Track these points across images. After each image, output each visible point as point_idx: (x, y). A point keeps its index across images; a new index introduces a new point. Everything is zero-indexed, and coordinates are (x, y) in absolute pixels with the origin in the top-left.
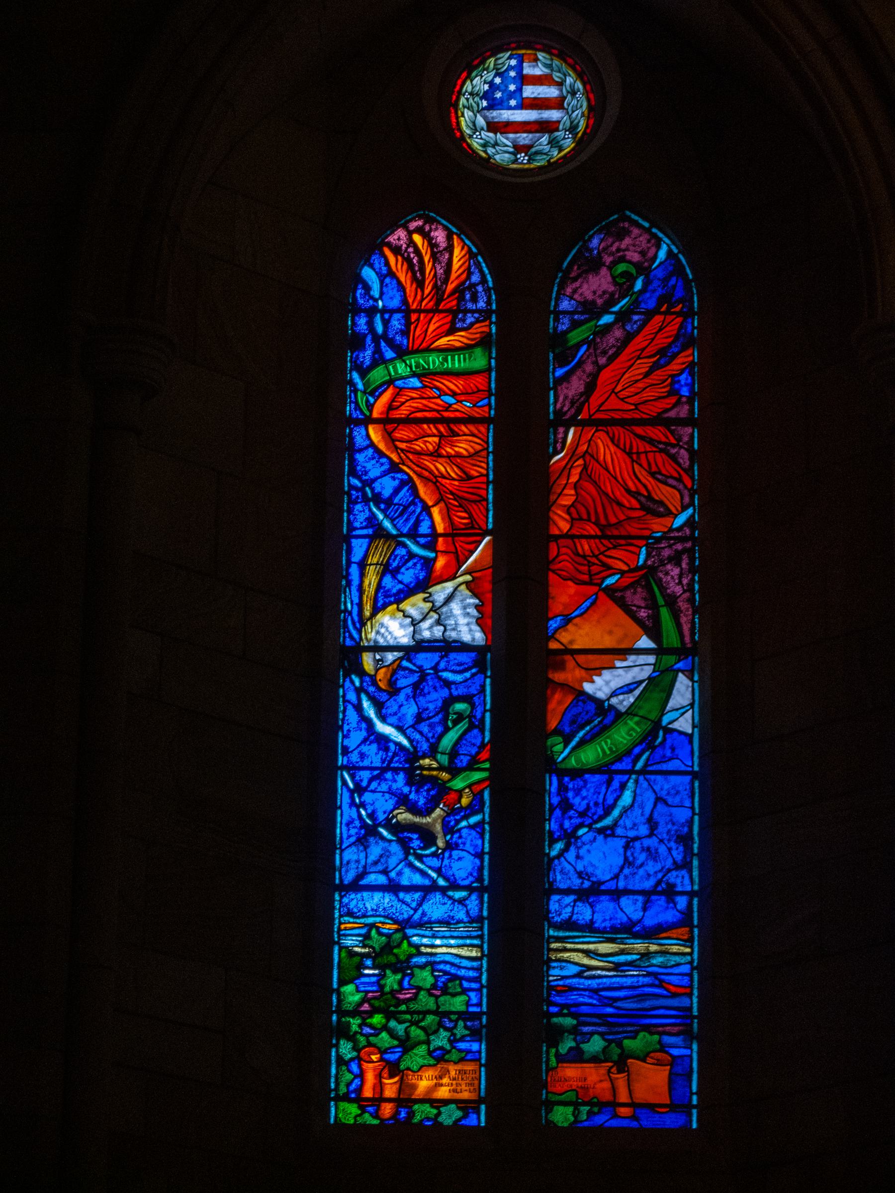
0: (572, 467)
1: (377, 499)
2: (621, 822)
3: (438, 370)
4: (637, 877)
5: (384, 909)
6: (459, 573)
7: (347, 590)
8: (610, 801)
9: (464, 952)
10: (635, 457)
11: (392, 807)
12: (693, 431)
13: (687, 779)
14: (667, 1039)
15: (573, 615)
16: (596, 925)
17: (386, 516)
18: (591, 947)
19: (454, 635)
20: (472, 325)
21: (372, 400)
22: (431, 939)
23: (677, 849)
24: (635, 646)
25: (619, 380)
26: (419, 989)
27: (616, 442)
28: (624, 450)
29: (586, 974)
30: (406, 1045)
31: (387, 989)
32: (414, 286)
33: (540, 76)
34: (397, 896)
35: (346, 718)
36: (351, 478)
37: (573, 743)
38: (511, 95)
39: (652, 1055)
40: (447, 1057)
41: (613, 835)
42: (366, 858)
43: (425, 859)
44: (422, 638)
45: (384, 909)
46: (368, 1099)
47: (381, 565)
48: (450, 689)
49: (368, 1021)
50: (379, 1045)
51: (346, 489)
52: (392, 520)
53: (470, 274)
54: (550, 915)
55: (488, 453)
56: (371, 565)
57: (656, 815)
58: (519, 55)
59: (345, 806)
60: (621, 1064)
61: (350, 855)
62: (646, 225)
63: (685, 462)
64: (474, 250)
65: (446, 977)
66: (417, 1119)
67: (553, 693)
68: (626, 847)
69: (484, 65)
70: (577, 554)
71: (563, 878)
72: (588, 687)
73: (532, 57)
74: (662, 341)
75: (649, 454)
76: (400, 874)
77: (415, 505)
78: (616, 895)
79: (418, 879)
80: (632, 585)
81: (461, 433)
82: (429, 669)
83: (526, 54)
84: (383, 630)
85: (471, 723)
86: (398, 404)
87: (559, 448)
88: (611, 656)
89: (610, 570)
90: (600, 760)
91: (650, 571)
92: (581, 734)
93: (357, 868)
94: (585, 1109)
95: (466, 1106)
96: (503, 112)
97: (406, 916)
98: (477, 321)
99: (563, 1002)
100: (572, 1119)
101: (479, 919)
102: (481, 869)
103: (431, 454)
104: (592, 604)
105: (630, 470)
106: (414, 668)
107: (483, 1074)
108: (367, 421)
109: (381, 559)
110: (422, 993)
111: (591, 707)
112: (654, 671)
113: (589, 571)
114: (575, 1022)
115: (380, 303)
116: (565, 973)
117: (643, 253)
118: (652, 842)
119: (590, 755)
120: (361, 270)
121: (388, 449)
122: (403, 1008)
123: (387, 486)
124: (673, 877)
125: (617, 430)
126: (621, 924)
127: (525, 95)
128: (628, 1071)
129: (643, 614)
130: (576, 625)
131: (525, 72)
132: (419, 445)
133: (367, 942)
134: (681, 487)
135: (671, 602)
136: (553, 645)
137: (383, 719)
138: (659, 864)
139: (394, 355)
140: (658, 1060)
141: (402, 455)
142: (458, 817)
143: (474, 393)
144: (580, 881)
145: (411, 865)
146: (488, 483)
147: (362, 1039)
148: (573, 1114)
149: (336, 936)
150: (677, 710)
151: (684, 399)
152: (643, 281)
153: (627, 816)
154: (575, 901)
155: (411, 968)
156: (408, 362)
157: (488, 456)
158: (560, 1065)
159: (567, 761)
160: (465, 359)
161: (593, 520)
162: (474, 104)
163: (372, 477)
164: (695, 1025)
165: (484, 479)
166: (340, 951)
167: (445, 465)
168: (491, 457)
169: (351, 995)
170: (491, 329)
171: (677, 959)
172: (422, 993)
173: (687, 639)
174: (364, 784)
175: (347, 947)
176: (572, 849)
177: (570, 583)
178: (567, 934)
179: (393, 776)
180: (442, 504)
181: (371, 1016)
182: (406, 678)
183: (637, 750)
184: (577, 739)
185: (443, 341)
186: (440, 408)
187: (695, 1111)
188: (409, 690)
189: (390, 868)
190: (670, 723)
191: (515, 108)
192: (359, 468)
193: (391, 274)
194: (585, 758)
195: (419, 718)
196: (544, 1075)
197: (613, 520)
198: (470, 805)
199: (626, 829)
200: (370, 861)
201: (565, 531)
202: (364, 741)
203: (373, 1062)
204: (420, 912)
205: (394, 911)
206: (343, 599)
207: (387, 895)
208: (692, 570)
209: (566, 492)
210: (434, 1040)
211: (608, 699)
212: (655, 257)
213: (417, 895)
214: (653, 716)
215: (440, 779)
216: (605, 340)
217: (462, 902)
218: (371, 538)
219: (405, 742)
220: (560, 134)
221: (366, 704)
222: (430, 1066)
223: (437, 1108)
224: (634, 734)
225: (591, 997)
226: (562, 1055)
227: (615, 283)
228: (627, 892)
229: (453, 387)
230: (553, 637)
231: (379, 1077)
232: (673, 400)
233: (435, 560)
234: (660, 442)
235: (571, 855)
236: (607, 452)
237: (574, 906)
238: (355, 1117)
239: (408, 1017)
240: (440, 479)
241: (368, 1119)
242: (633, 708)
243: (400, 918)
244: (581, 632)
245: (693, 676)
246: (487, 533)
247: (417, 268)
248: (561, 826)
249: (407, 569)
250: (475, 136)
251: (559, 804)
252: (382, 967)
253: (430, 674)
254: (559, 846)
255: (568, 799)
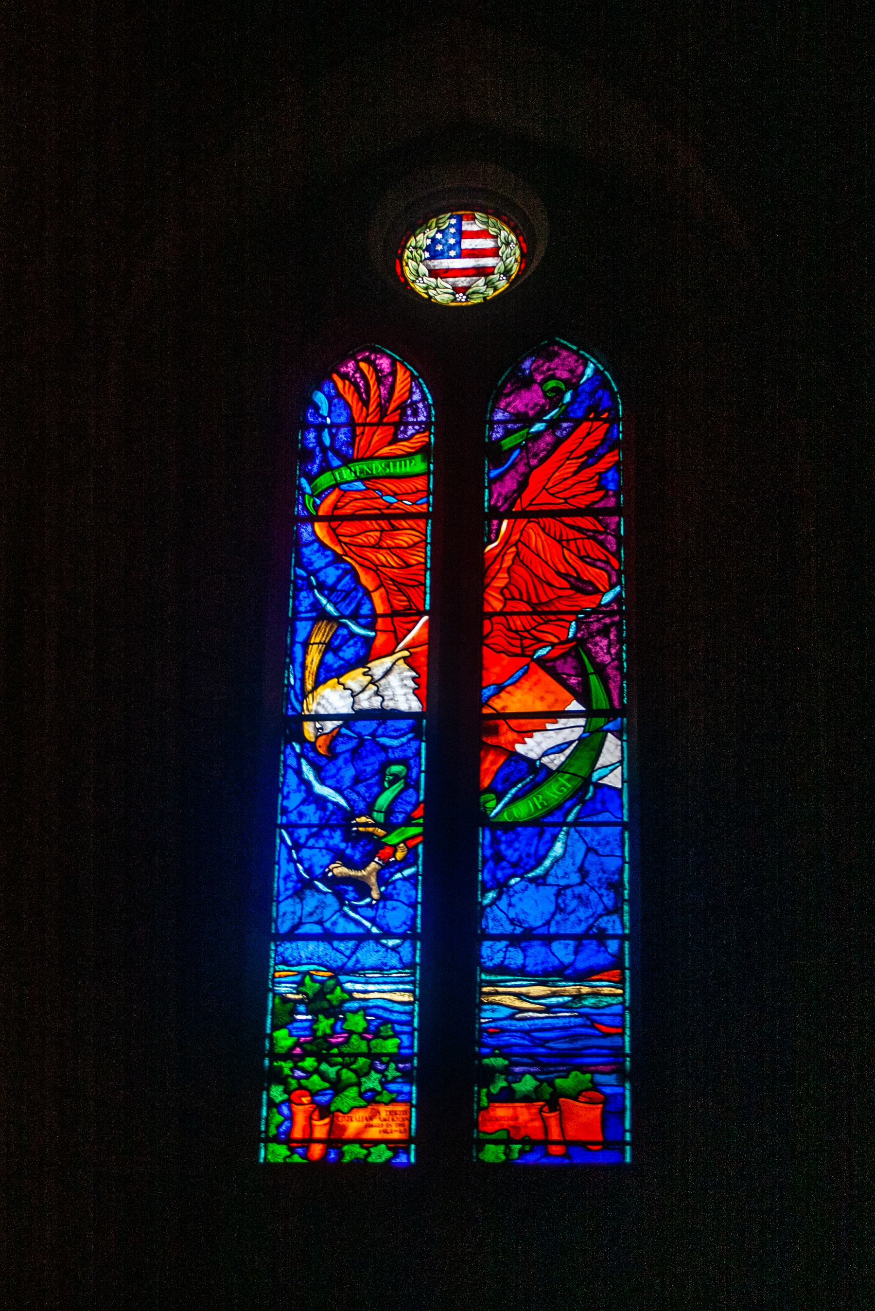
0: (505, 553)
1: (322, 586)
2: (553, 871)
3: (381, 475)
4: (569, 923)
5: (319, 957)
6: (397, 650)
7: (291, 667)
8: (542, 852)
9: (397, 997)
10: (564, 543)
11: (328, 862)
12: (620, 520)
13: (618, 829)
14: (599, 1078)
15: (506, 684)
16: (528, 969)
17: (329, 601)
18: (523, 990)
19: (389, 705)
20: (412, 435)
21: (318, 501)
22: (363, 985)
23: (608, 895)
24: (566, 709)
25: (549, 479)
26: (351, 1033)
27: (547, 531)
28: (555, 538)
29: (518, 1016)
30: (337, 1087)
31: (319, 1033)
32: (360, 405)
33: (478, 231)
34: (332, 945)
35: (287, 781)
36: (296, 569)
37: (506, 799)
38: (451, 247)
39: (584, 1093)
40: (378, 1098)
41: (545, 884)
42: (302, 909)
43: (359, 910)
44: (361, 708)
45: (319, 957)
46: (297, 1141)
47: (324, 643)
48: (387, 753)
49: (300, 1064)
50: (310, 1087)
51: (292, 578)
52: (335, 605)
53: (411, 393)
54: (483, 960)
55: (427, 544)
56: (314, 643)
57: (586, 864)
58: (459, 215)
59: (283, 862)
60: (553, 1103)
61: (286, 906)
62: (575, 348)
63: (612, 547)
64: (416, 373)
65: (379, 1021)
66: (347, 1159)
67: (486, 755)
68: (558, 895)
69: (427, 224)
70: (510, 629)
71: (495, 925)
72: (520, 748)
73: (470, 217)
74: (590, 444)
75: (578, 541)
76: (334, 923)
77: (357, 592)
78: (548, 940)
79: (352, 928)
80: (563, 656)
81: (401, 527)
82: (367, 735)
83: (464, 214)
84: (323, 702)
85: (406, 783)
86: (343, 504)
87: (493, 538)
88: (543, 720)
89: (543, 643)
90: (533, 814)
91: (580, 642)
92: (513, 791)
93: (293, 919)
94: (517, 1147)
95: (397, 1147)
96: (442, 261)
97: (340, 963)
98: (418, 432)
99: (495, 1043)
100: (503, 1157)
101: (412, 965)
102: (414, 917)
103: (373, 547)
104: (524, 674)
105: (561, 553)
106: (353, 735)
107: (414, 1114)
108: (311, 519)
109: (324, 639)
110: (354, 1038)
111: (523, 766)
112: (584, 732)
113: (522, 644)
114: (506, 1062)
115: (328, 421)
116: (496, 1015)
117: (571, 371)
118: (583, 890)
119: (522, 810)
120: (311, 393)
121: (333, 542)
122: (335, 1051)
123: (331, 575)
124: (604, 922)
125: (548, 521)
126: (553, 967)
127: (463, 247)
128: (560, 1110)
129: (573, 681)
130: (509, 693)
131: (464, 228)
132: (361, 539)
133: (302, 989)
134: (609, 568)
135: (600, 670)
136: (486, 711)
137: (322, 781)
138: (590, 910)
139: (339, 463)
140: (590, 1098)
141: (345, 547)
142: (392, 870)
143: (414, 493)
144: (512, 927)
145: (346, 916)
146: (426, 569)
147: (293, 1082)
148: (505, 1154)
149: (270, 983)
150: (606, 767)
151: (611, 493)
152: (571, 395)
153: (559, 866)
154: (507, 947)
155: (343, 1013)
156: (353, 469)
157: (426, 546)
158: (491, 1104)
159: (499, 816)
160: (405, 465)
161: (525, 598)
162: (418, 257)
163: (317, 567)
164: (628, 1063)
165: (423, 566)
166: (274, 997)
167: (386, 555)
168: (429, 547)
169: (284, 1039)
170: (430, 439)
171: (609, 1000)
172: (355, 1036)
173: (616, 703)
174: (302, 840)
175: (281, 994)
176: (504, 897)
177: (504, 656)
178: (499, 978)
179: (331, 833)
180: (382, 590)
181: (303, 1060)
182: (345, 743)
183: (568, 805)
184: (509, 796)
185: (386, 450)
186: (381, 507)
187: (628, 1148)
188: (347, 755)
189: (326, 918)
190: (601, 779)
191: (455, 257)
192: (305, 560)
193: (339, 395)
194: (517, 813)
195: (357, 780)
196: (475, 1115)
197: (544, 599)
198: (405, 859)
199: (558, 878)
200: (305, 912)
201: (498, 609)
202: (303, 803)
203: (303, 1104)
204: (354, 959)
205: (328, 959)
206: (286, 675)
207: (321, 943)
208: (620, 641)
209: (500, 575)
210: (365, 1082)
211: (540, 759)
212: (583, 374)
213: (351, 944)
214: (583, 773)
215: (376, 836)
216: (536, 445)
217: (394, 949)
218: (315, 621)
219: (343, 802)
220: (495, 277)
221: (306, 768)
222: (361, 1107)
223: (367, 1148)
224: (565, 790)
225: (523, 1038)
226: (493, 1095)
227: (546, 397)
228: (558, 937)
229: (394, 488)
230: (486, 704)
231: (309, 1118)
232: (601, 493)
233: (374, 638)
234: (589, 530)
235: (503, 903)
236: (539, 540)
237: (505, 952)
238: (285, 1159)
239: (340, 1060)
240: (380, 568)
241: (296, 1158)
242: (563, 767)
243: (334, 965)
244: (514, 699)
245: (622, 735)
246: (425, 613)
247: (362, 390)
248: (494, 876)
249: (349, 647)
250: (417, 281)
251: (492, 855)
252: (315, 1013)
253: (367, 740)
254: (491, 895)
255: (500, 851)
